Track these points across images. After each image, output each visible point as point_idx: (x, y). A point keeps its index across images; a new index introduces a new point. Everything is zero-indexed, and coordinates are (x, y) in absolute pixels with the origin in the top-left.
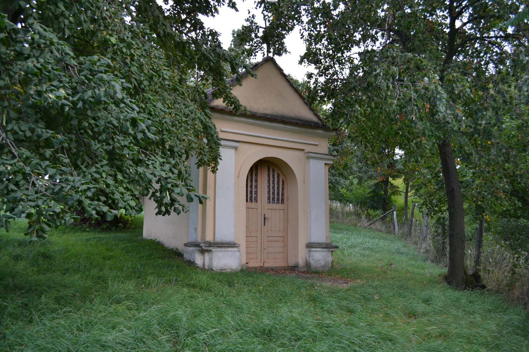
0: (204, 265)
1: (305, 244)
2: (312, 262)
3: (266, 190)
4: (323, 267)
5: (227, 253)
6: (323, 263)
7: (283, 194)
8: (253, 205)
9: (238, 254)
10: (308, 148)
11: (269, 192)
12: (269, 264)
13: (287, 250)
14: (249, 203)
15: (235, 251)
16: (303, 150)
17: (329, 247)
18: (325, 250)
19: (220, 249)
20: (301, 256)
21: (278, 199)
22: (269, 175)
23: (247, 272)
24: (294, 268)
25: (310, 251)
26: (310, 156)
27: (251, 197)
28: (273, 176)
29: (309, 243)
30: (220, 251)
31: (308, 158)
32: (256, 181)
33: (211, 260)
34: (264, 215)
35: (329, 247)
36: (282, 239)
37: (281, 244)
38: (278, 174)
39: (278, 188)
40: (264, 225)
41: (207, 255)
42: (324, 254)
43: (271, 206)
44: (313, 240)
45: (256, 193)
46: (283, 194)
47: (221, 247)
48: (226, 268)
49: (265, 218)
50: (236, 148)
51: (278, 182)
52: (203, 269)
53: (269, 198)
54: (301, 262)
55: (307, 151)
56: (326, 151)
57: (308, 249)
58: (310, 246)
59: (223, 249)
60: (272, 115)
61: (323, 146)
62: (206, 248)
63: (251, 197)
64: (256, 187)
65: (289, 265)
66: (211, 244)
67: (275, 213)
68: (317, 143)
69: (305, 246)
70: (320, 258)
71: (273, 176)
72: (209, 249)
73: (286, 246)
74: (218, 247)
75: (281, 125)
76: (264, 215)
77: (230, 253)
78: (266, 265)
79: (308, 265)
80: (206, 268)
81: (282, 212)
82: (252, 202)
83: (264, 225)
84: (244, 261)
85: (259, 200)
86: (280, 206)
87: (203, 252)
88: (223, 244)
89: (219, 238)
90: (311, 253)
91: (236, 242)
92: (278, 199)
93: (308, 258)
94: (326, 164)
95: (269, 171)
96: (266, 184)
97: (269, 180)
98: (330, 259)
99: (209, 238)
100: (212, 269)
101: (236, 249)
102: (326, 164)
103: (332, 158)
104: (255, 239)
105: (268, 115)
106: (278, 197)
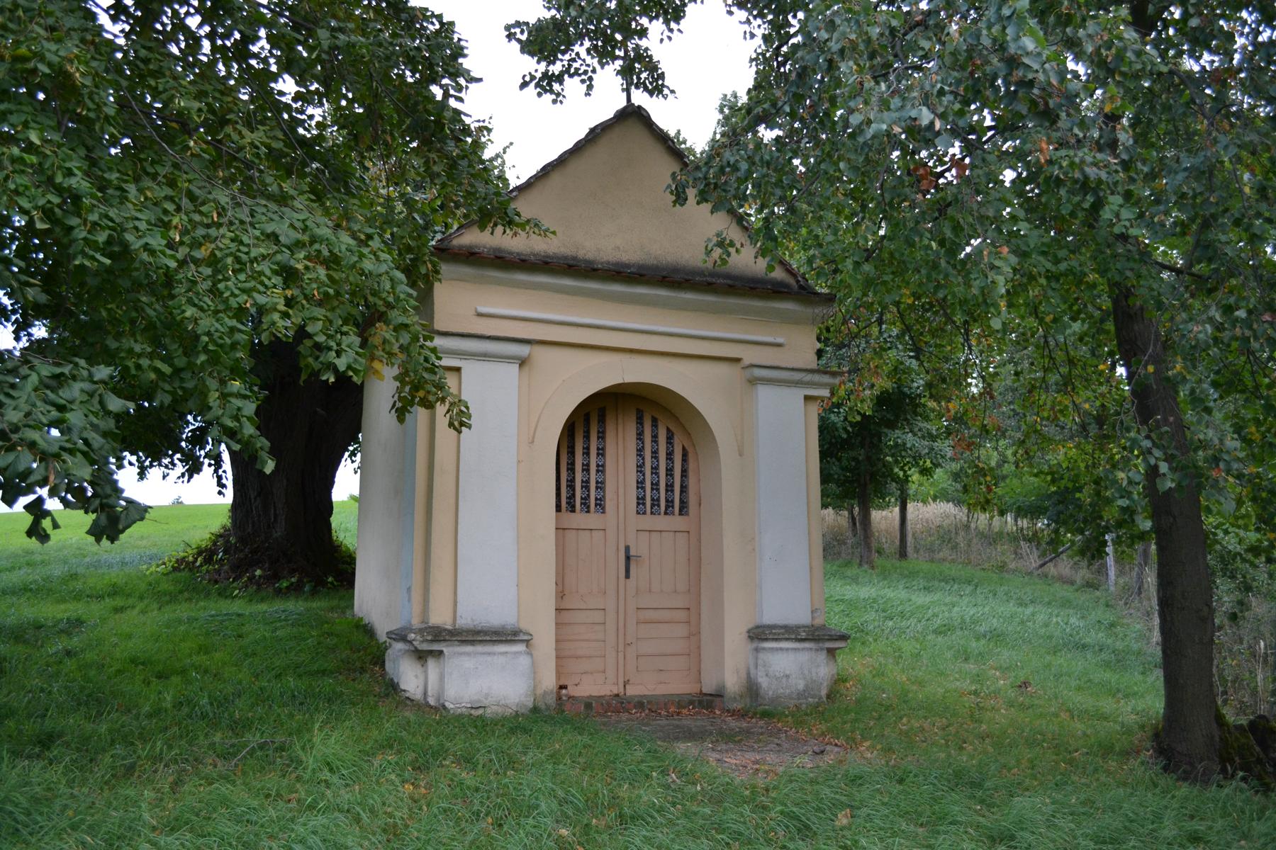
0: (425, 694)
1: (745, 629)
2: (763, 681)
3: (632, 477)
4: (801, 695)
5: (489, 659)
6: (801, 686)
7: (684, 489)
8: (578, 519)
9: (525, 661)
10: (750, 355)
11: (640, 484)
12: (644, 686)
13: (699, 647)
14: (565, 515)
15: (516, 653)
16: (738, 360)
17: (817, 636)
18: (807, 645)
19: (469, 649)
20: (730, 667)
21: (670, 503)
22: (640, 436)
23: (556, 715)
24: (708, 701)
25: (757, 650)
26: (756, 377)
27: (572, 497)
28: (655, 438)
29: (758, 627)
30: (468, 654)
31: (753, 381)
32: (601, 452)
33: (442, 678)
34: (627, 549)
35: (817, 636)
36: (682, 615)
37: (681, 630)
38: (668, 430)
39: (670, 472)
40: (627, 576)
41: (431, 663)
42: (804, 657)
43: (648, 521)
44: (773, 615)
45: (601, 486)
46: (684, 489)
47: (472, 642)
48: (486, 703)
49: (628, 558)
50: (523, 362)
51: (670, 456)
52: (422, 707)
53: (641, 501)
54: (732, 682)
55: (746, 361)
56: (810, 360)
57: (755, 645)
58: (759, 634)
59: (479, 648)
60: (641, 267)
61: (799, 346)
62: (425, 647)
63: (574, 492)
64: (601, 469)
65: (704, 691)
66: (438, 634)
67: (659, 539)
68: (780, 340)
69: (745, 635)
70: (790, 670)
71: (655, 438)
72: (435, 647)
73: (694, 634)
74: (464, 642)
75: (663, 293)
76: (627, 549)
77: (502, 659)
78: (632, 691)
79: (752, 689)
80: (432, 701)
81: (682, 538)
82: (573, 511)
83: (627, 576)
84: (549, 681)
85: (609, 505)
86: (676, 521)
87: (422, 656)
88: (478, 632)
89: (469, 616)
90: (761, 655)
91: (524, 626)
92: (670, 503)
93: (753, 671)
94: (807, 398)
95: (640, 421)
96: (632, 460)
97: (640, 452)
98: (835, 671)
99: (440, 617)
100: (444, 707)
101: (521, 648)
102: (807, 398)
103: (826, 379)
104: (598, 617)
105: (628, 266)
106: (672, 494)
